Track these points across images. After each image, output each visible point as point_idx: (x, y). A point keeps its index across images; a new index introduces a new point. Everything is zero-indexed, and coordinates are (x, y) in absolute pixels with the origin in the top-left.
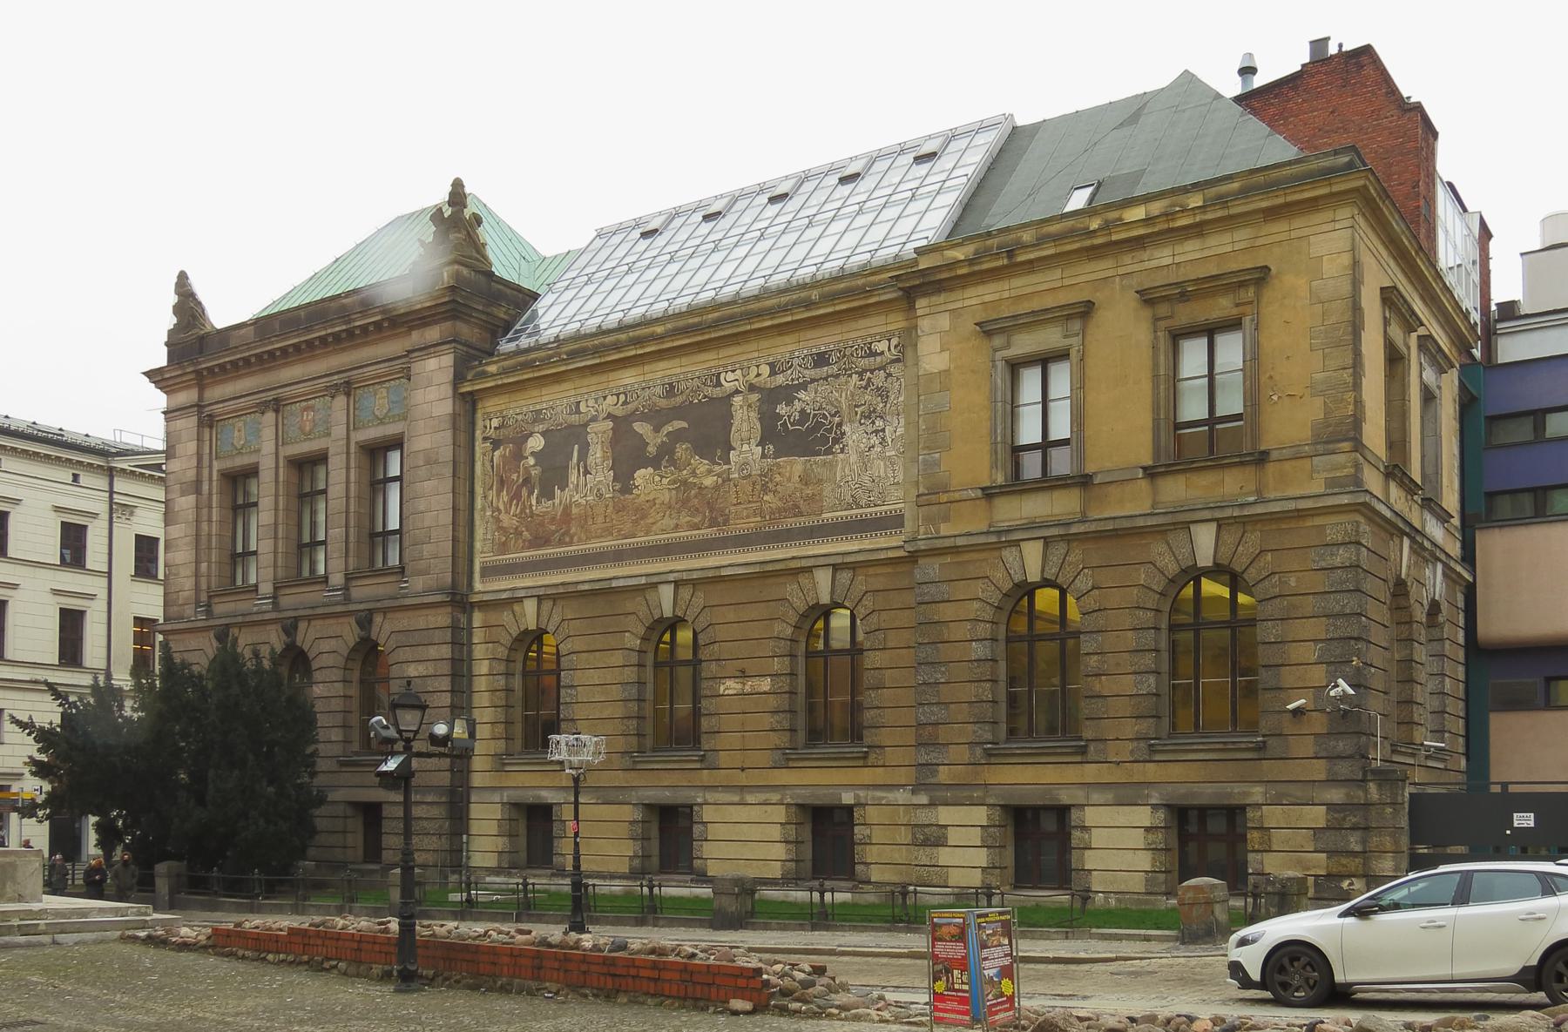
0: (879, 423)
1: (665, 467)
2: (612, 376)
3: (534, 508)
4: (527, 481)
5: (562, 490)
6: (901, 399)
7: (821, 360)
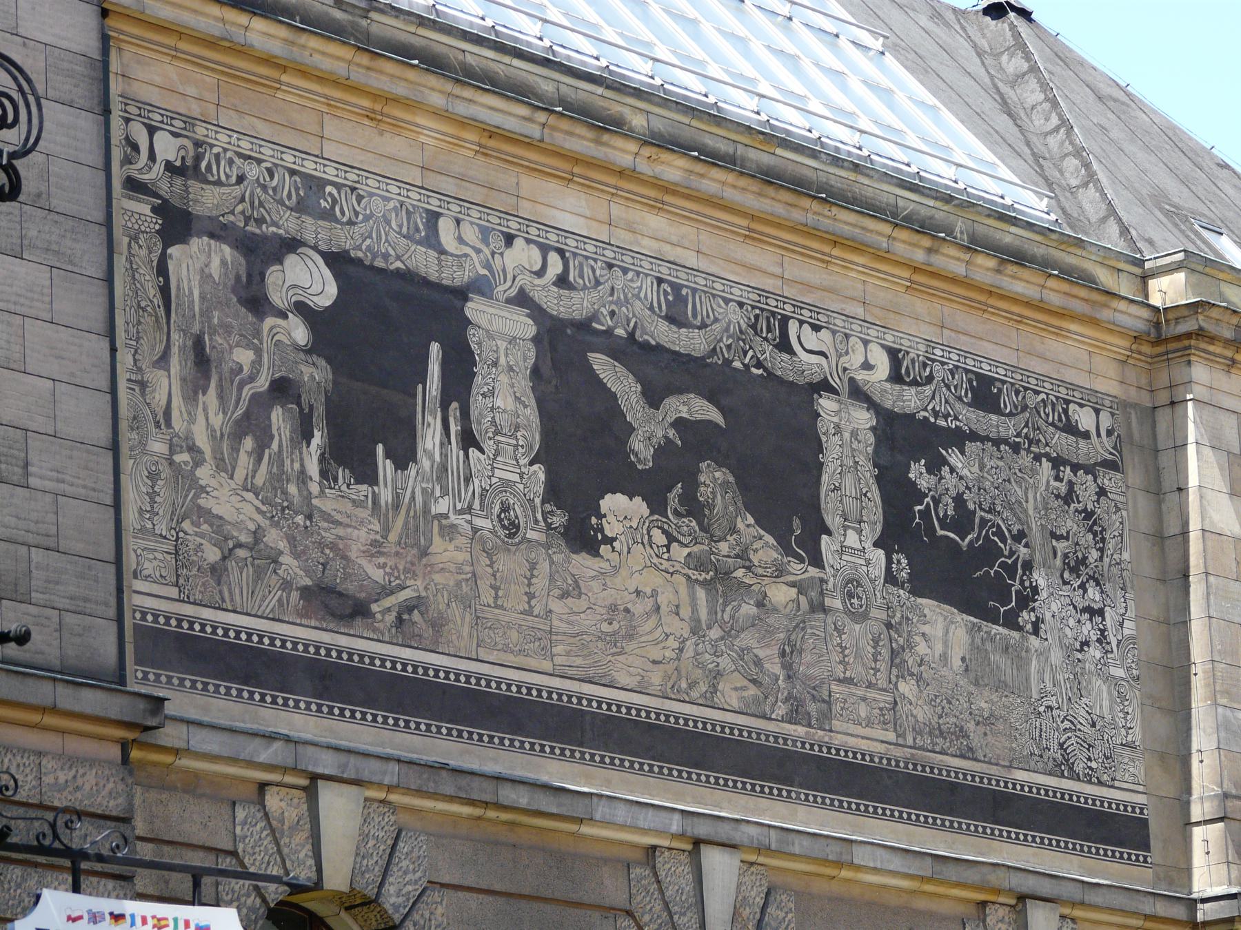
0: (1093, 592)
1: (677, 514)
2: (529, 183)
3: (314, 488)
6: (1126, 556)
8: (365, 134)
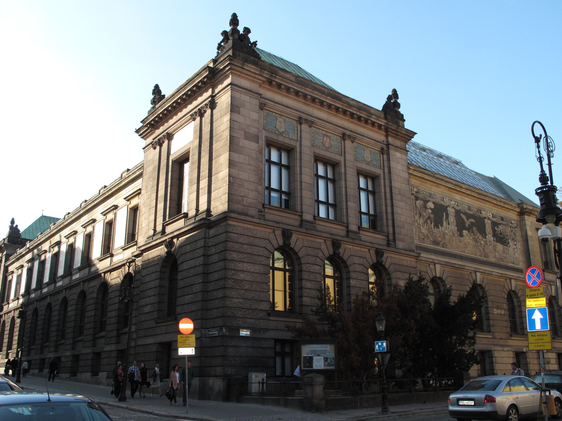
0: (515, 242)
2: (453, 194)
4: (429, 218)
5: (442, 227)
7: (502, 219)
8: (436, 188)
